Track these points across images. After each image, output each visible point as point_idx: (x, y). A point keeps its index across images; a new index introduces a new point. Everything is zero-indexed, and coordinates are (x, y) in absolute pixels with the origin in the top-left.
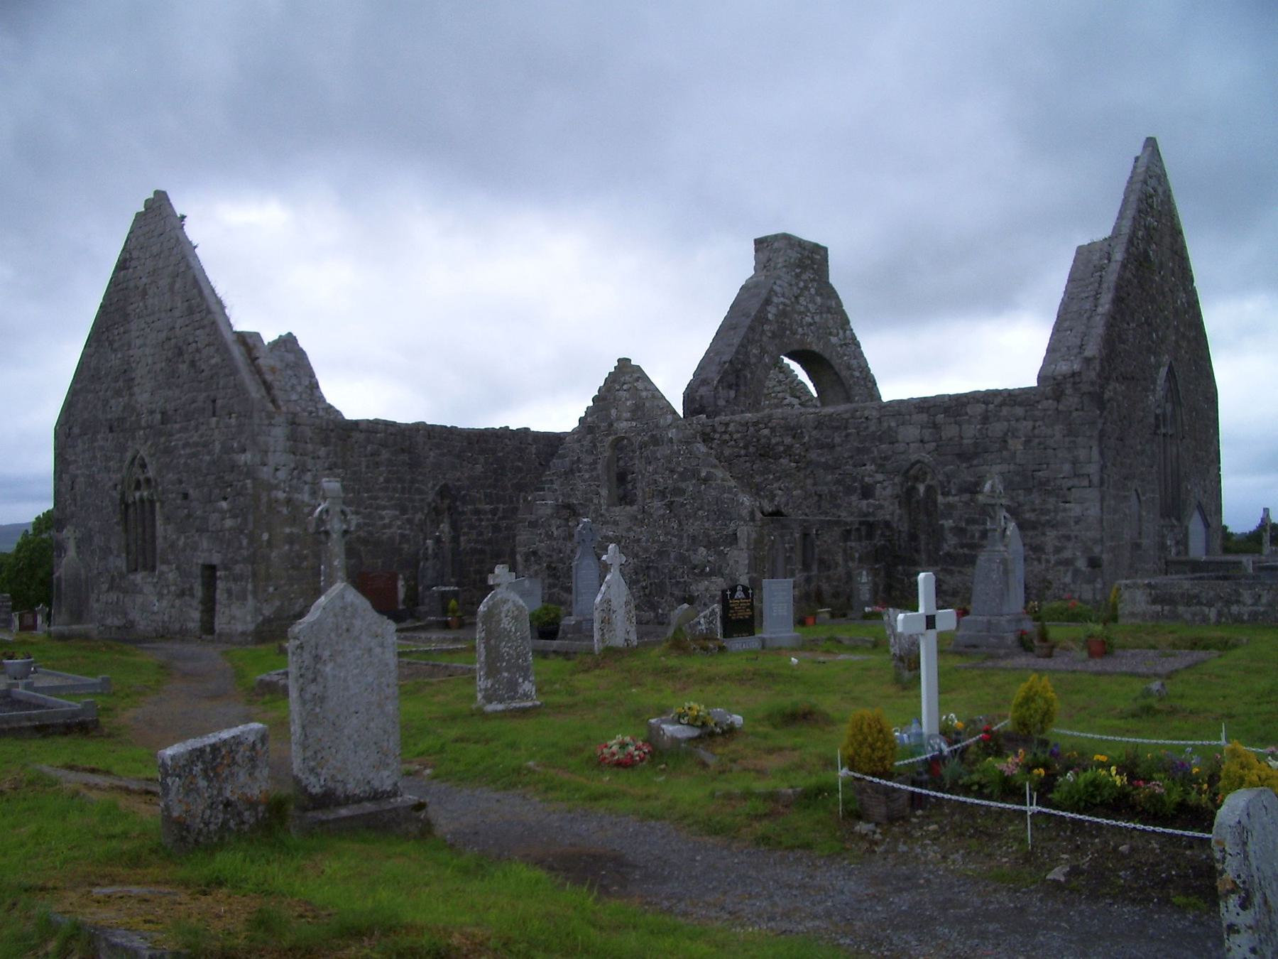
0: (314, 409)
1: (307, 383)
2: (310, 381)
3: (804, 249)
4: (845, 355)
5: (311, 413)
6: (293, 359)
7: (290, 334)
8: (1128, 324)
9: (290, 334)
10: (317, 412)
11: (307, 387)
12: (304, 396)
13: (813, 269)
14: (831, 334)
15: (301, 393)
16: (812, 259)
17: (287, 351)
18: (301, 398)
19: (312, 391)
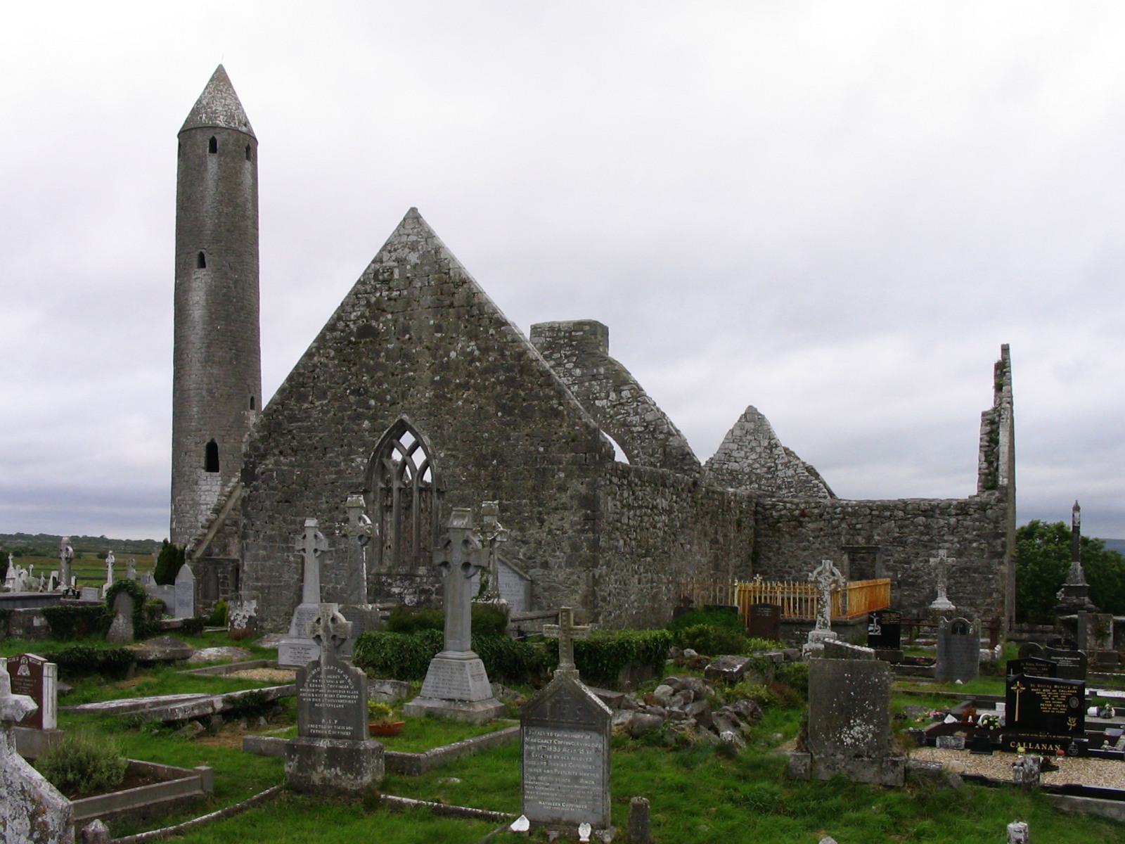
0: (773, 465)
1: (766, 444)
2: (769, 443)
3: (559, 330)
4: (621, 414)
5: (770, 468)
6: (753, 427)
7: (750, 407)
8: (312, 403)
9: (750, 407)
10: (777, 467)
11: (766, 448)
12: (763, 455)
13: (572, 345)
14: (596, 398)
15: (760, 453)
16: (571, 339)
17: (747, 421)
18: (760, 457)
19: (771, 451)
